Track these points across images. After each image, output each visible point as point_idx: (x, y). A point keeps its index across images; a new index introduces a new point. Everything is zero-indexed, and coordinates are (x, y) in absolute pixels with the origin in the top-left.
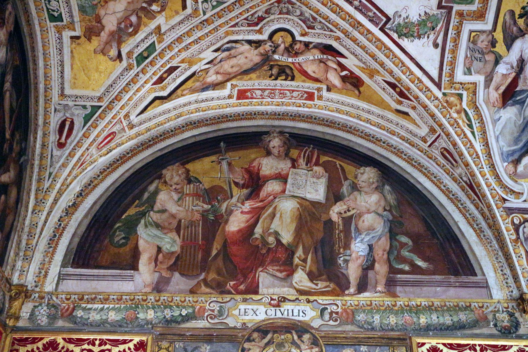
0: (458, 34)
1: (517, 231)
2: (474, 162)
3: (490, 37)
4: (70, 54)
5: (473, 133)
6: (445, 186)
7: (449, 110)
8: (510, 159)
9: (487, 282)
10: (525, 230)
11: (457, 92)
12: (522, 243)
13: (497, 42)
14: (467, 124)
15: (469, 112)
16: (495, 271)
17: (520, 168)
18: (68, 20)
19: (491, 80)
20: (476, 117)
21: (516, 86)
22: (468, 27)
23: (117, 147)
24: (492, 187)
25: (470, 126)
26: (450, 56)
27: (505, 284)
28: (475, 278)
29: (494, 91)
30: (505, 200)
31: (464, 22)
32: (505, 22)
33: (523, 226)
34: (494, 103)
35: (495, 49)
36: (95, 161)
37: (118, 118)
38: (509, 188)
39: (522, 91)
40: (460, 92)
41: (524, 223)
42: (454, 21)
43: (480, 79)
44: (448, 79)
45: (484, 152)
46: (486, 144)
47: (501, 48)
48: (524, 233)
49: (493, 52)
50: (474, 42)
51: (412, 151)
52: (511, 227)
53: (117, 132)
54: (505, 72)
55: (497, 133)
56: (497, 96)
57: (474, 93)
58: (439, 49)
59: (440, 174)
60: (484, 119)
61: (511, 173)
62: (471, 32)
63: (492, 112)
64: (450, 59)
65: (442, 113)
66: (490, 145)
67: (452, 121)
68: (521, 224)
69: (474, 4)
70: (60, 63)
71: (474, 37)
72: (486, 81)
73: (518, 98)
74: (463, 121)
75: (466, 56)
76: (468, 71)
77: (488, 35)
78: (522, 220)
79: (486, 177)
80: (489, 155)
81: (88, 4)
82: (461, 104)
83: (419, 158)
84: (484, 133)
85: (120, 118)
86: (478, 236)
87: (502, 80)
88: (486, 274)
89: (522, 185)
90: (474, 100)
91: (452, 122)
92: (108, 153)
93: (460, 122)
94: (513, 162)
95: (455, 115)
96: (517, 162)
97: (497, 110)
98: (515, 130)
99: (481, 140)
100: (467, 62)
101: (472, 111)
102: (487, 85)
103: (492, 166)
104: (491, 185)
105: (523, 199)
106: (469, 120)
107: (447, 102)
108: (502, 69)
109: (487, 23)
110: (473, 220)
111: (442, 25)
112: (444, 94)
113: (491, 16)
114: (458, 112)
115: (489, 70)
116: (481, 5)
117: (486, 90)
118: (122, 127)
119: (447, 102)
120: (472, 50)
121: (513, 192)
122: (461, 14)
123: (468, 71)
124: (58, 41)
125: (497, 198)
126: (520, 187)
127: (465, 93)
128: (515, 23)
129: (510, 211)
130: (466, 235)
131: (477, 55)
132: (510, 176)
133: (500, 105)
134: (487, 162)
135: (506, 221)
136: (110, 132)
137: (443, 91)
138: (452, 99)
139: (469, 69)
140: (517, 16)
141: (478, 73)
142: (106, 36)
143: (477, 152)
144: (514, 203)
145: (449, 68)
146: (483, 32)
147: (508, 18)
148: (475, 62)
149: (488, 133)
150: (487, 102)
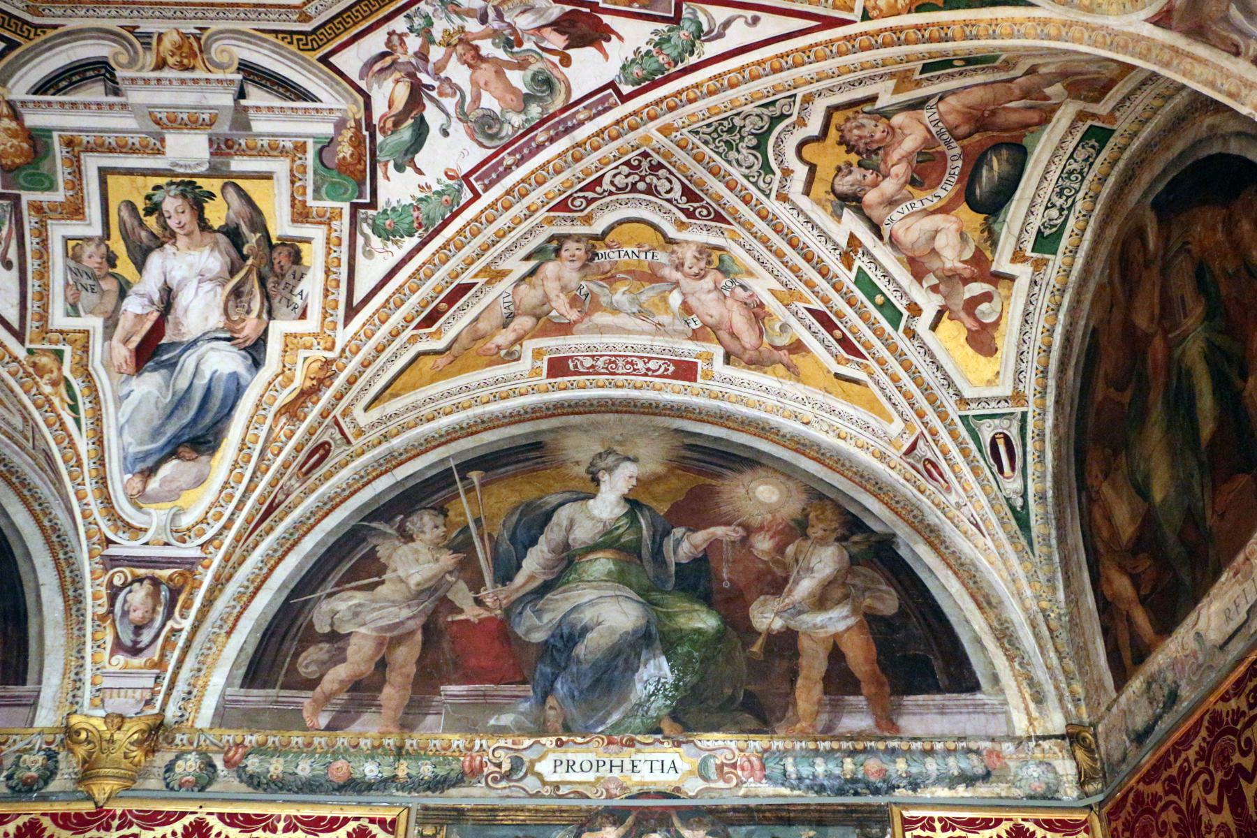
0: (44, 243)
1: (112, 599)
2: (70, 473)
3: (103, 249)
5: (77, 421)
6: (50, 521)
7: (38, 379)
8: (139, 467)
9: (38, 696)
10: (129, 597)
11: (54, 347)
12: (114, 621)
13: (116, 257)
14: (69, 406)
15: (74, 383)
16: (64, 674)
17: (154, 484)
19: (115, 325)
20: (86, 392)
21: (162, 335)
22: (59, 231)
24: (91, 519)
25: (74, 408)
26: (37, 283)
27: (70, 699)
28: (21, 688)
29: (121, 345)
30: (109, 542)
31: (49, 222)
32: (122, 223)
33: (127, 589)
34: (120, 367)
35: (115, 271)
38: (123, 521)
39: (173, 345)
40: (60, 347)
41: (131, 584)
42: (29, 222)
43: (95, 323)
44: (37, 324)
45: (93, 454)
46: (99, 441)
47: (125, 267)
48: (125, 601)
49: (113, 276)
50: (76, 258)
51: (21, 457)
52: (104, 591)
54: (139, 311)
55: (122, 421)
56: (127, 354)
57: (85, 349)
58: (15, 272)
59: (51, 499)
60: (101, 394)
61: (135, 492)
62: (66, 240)
63: (115, 383)
64: (37, 288)
65: (22, 386)
66: (106, 443)
67: (41, 400)
68: (125, 585)
69: (57, 190)
71: (73, 248)
72: (106, 327)
73: (165, 357)
74: (62, 400)
75: (67, 284)
76: (73, 310)
77: (98, 246)
78: (130, 579)
79: (85, 501)
80: (101, 461)
82: (60, 369)
83: (27, 470)
84: (98, 420)
86: (68, 609)
87: (135, 325)
88: (44, 681)
89: (149, 514)
90: (84, 362)
91: (40, 402)
93: (56, 401)
94: (142, 472)
95: (47, 389)
96: (150, 472)
97: (127, 379)
98: (156, 413)
99: (91, 434)
100: (69, 293)
101: (81, 380)
102: (108, 335)
103: (102, 481)
104: (91, 515)
105: (144, 540)
106: (73, 397)
107: (34, 365)
108: (133, 305)
109: (90, 224)
110: (73, 582)
111: (10, 228)
112: (30, 352)
113: (93, 209)
114: (54, 384)
115: (110, 307)
116: (71, 193)
117: (106, 344)
119: (34, 365)
120: (76, 273)
121: (128, 527)
122: (38, 208)
123: (73, 310)
125: (95, 539)
126: (145, 518)
127: (68, 350)
128: (141, 224)
129: (113, 562)
130: (45, 609)
131: (86, 281)
132: (132, 500)
133: (131, 369)
134: (94, 473)
135: (98, 582)
137: (28, 345)
138: (44, 360)
139: (74, 306)
140: (142, 213)
141: (91, 312)
143: (78, 456)
144: (127, 547)
145: (38, 304)
146: (89, 239)
147: (125, 214)
148: (84, 293)
149: (104, 420)
150: (107, 365)
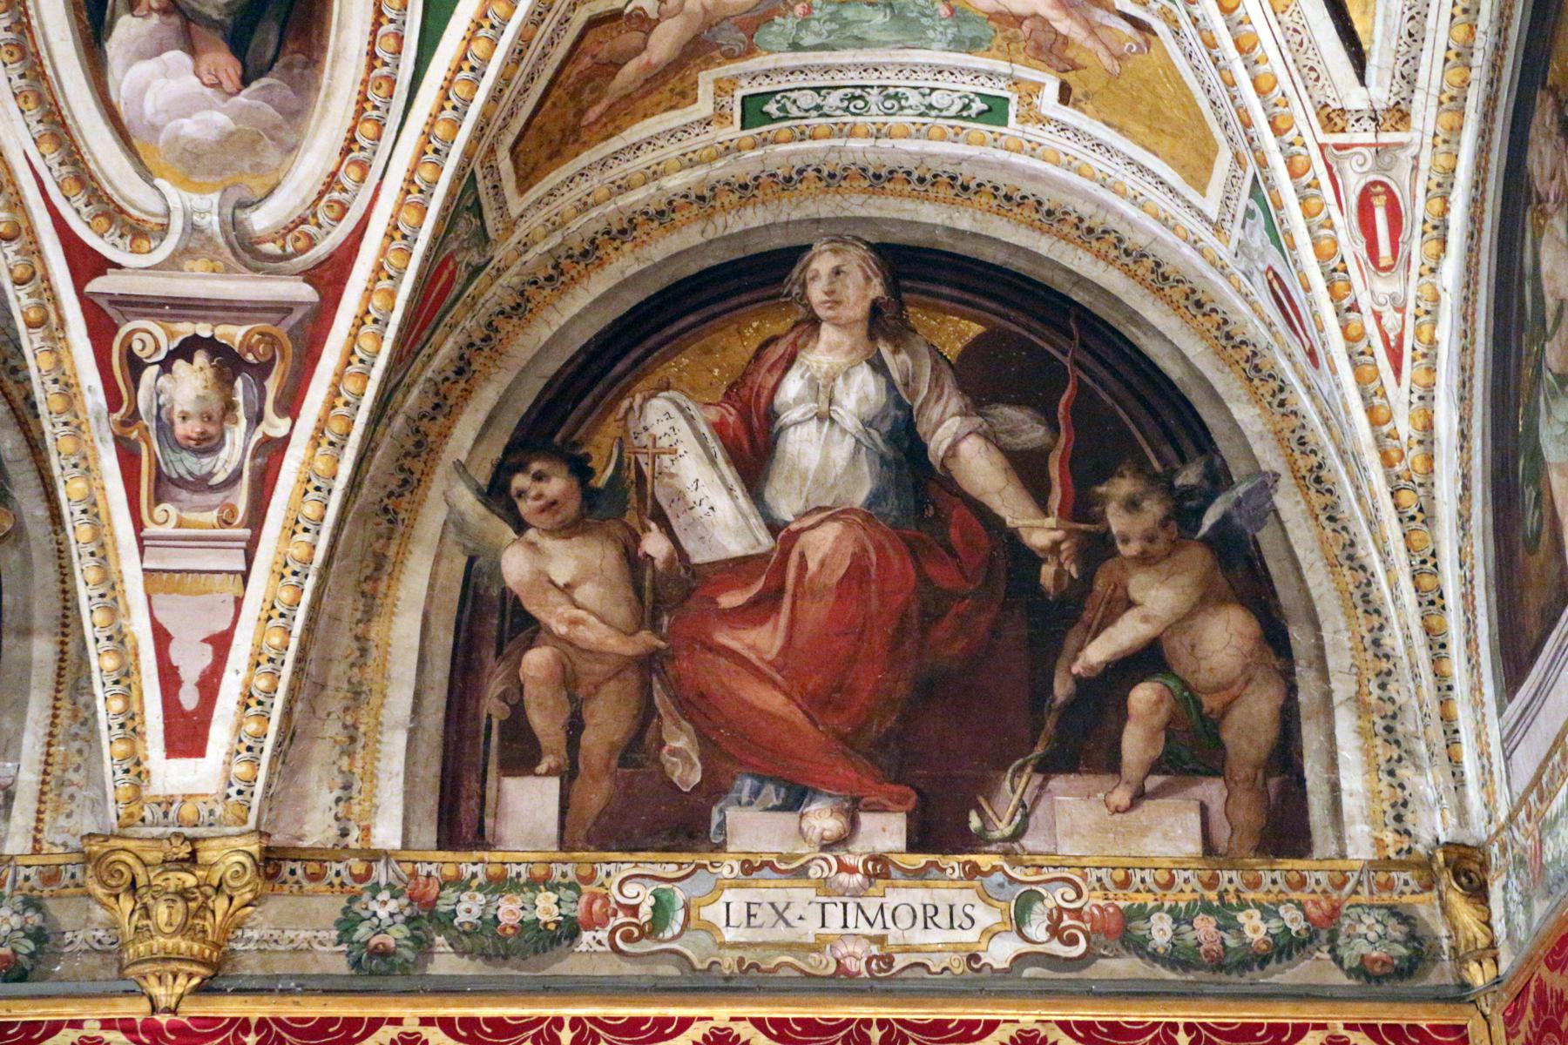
4: (1113, 132)
18: (1003, 85)
23: (1445, 199)
36: (1436, 299)
37: (1315, 153)
53: (1372, 177)
70: (1134, 169)
81: (946, 27)
85: (1322, 147)
92: (1444, 242)
118: (1369, 153)
124: (1070, 134)
136: (1353, 200)
142: (1068, 22)
